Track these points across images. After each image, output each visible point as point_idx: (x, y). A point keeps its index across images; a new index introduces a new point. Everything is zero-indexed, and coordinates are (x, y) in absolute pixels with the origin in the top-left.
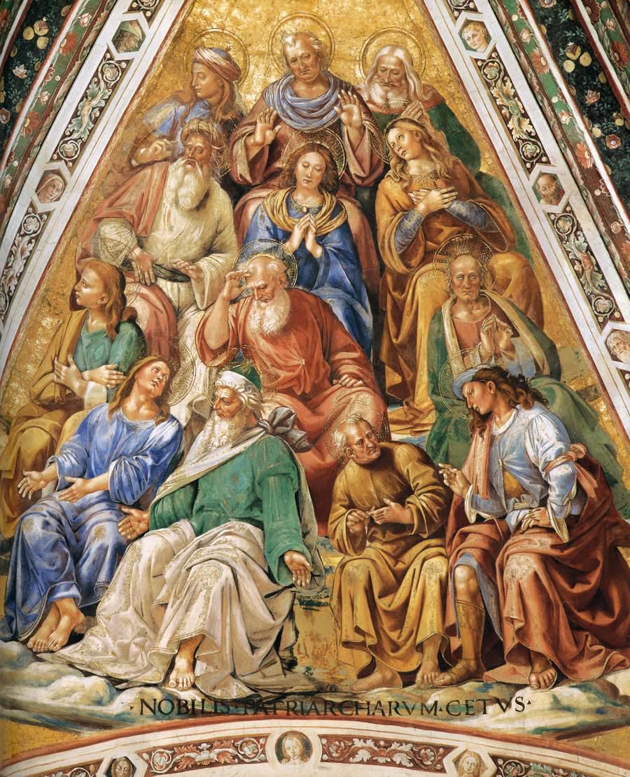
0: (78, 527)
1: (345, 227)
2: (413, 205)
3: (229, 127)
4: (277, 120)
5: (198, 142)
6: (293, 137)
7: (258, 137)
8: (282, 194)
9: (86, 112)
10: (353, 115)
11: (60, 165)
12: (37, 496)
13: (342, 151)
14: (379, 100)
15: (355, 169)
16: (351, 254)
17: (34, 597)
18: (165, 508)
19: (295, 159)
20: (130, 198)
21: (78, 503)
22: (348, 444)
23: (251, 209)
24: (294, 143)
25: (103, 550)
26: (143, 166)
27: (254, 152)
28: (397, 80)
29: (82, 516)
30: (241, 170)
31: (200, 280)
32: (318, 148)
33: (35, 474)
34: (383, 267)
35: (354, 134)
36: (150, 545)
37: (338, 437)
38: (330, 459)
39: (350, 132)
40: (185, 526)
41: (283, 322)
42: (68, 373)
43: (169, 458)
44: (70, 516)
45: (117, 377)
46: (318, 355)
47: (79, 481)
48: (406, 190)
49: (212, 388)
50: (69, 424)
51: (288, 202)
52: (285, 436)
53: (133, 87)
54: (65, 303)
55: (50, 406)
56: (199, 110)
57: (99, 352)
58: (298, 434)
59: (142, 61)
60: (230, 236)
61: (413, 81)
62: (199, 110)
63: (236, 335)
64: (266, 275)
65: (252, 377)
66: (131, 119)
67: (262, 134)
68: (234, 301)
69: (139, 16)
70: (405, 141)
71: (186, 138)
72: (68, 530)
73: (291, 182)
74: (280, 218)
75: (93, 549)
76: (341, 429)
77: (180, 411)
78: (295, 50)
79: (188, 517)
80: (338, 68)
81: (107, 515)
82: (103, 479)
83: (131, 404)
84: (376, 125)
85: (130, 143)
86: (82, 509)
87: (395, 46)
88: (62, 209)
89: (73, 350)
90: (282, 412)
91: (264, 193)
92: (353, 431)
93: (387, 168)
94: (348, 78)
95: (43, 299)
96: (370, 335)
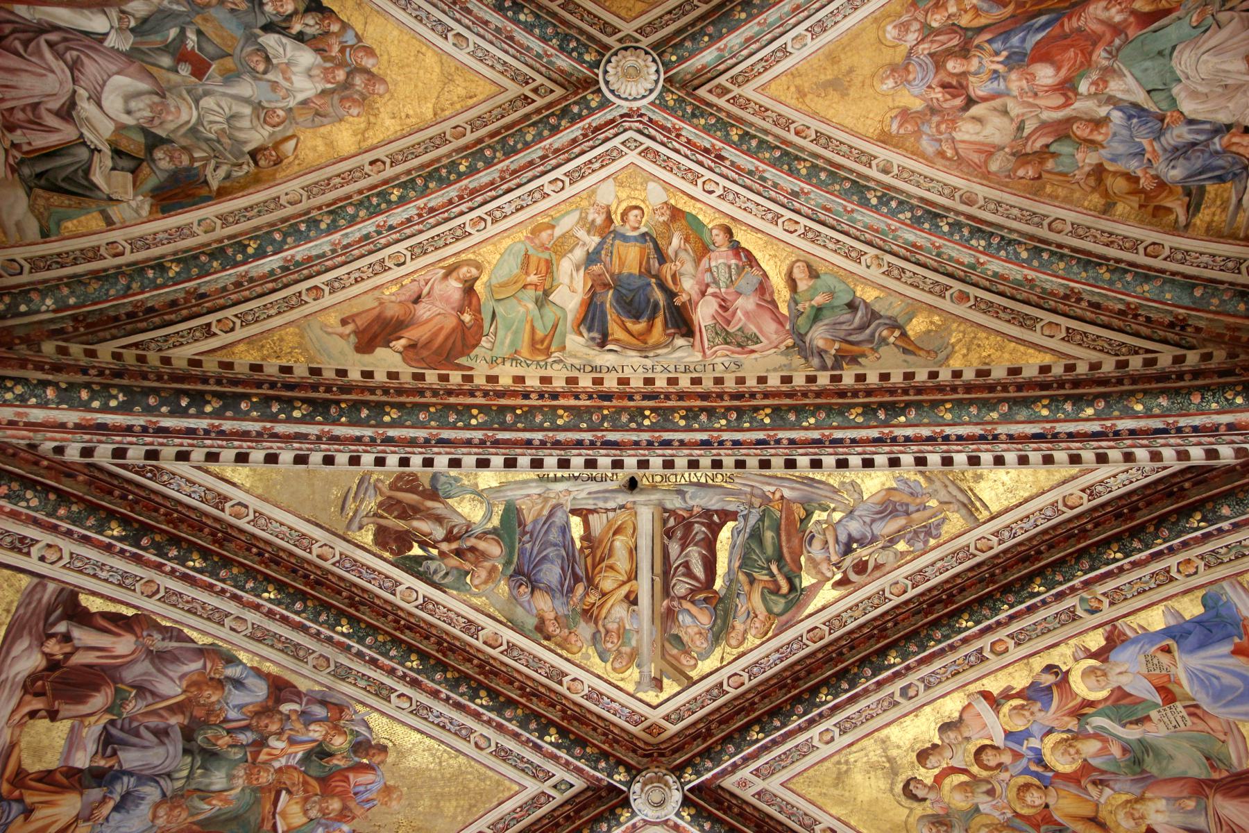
0: (1176, 149)
1: (989, 41)
2: (974, 7)
3: (933, 111)
4: (930, 87)
5: (943, 127)
6: (939, 77)
7: (940, 96)
8: (971, 79)
9: (927, 185)
10: (925, 48)
11: (957, 196)
12: (1156, 177)
13: (947, 50)
14: (916, 35)
15: (955, 42)
16: (1006, 35)
17: (1220, 162)
18: (1164, 105)
19: (950, 74)
20: (976, 158)
21: (1160, 152)
22: (1122, 11)
23: (981, 93)
24: (942, 76)
25: (1190, 132)
26: (957, 153)
27: (948, 97)
28: (904, 27)
29: (1169, 148)
30: (959, 102)
31: (1023, 114)
32: (944, 62)
33: (1142, 181)
34: (1012, 16)
35: (935, 46)
36: (1188, 107)
37: (1118, 18)
38: (1132, 19)
39: (935, 48)
40: (1176, 90)
41: (1048, 65)
42: (1079, 175)
43: (1135, 111)
44: (1168, 155)
45: (1082, 148)
46: (1068, 41)
47: (1147, 156)
48: (966, 11)
49: (1090, 96)
50: (1111, 168)
51: (976, 74)
52: (1118, 50)
53: (912, 162)
54: (1037, 183)
55: (1100, 181)
56: (925, 128)
57: (1067, 161)
58: (1117, 42)
59: (897, 159)
60: (997, 103)
61: (905, 18)
62: (925, 128)
63: (1054, 90)
64: (1020, 80)
65: (1081, 76)
66: (929, 161)
67: (938, 94)
68: (1036, 94)
69: (874, 163)
70: (938, 17)
71: (941, 133)
72: (1177, 154)
73: (964, 74)
74: (985, 77)
75: (1190, 137)
76: (1111, 18)
77: (1103, 112)
78: (890, 83)
79: (1169, 90)
80: (899, 59)
81: (1168, 136)
82: (1145, 143)
83: (1099, 138)
84: (929, 35)
85: (944, 162)
86: (1165, 150)
87: (884, 31)
88: (981, 191)
89: (1065, 175)
90: (1104, 54)
91: (971, 88)
92: (1113, 11)
93: (953, 24)
94: (905, 53)
95: (1035, 194)
96: (1053, 15)
